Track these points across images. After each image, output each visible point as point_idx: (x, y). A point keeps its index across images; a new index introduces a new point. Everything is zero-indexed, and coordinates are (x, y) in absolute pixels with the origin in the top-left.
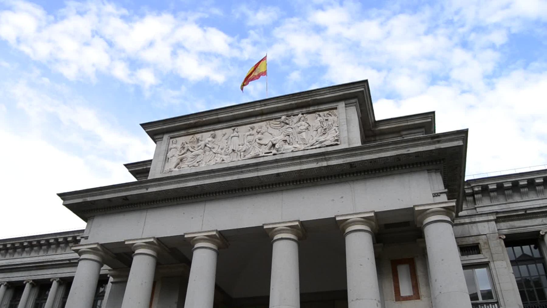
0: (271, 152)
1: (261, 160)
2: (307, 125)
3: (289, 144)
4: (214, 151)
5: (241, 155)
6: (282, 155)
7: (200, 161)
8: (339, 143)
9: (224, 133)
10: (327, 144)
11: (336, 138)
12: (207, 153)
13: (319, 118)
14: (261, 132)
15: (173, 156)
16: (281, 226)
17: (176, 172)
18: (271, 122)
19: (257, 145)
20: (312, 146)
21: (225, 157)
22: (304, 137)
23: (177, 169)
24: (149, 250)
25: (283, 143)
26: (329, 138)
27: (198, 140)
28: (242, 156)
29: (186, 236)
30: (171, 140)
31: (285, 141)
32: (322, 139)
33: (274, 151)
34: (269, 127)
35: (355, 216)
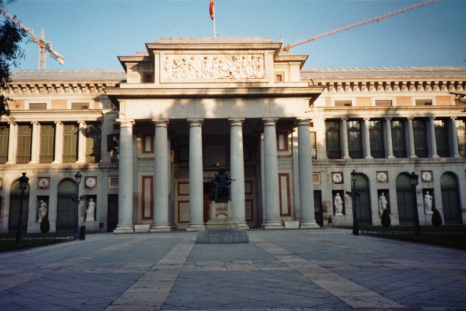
0: (229, 77)
1: (224, 81)
2: (248, 62)
3: (238, 73)
4: (196, 69)
5: (212, 75)
6: (235, 79)
7: (187, 75)
8: (264, 77)
9: (200, 58)
10: (258, 77)
11: (264, 75)
12: (192, 70)
13: (254, 60)
14: (223, 62)
15: (169, 68)
16: (236, 120)
17: (173, 80)
18: (228, 55)
19: (221, 70)
20: (251, 76)
21: (203, 75)
22: (247, 71)
23: (172, 78)
24: (164, 124)
25: (235, 72)
26: (260, 74)
27: (184, 60)
28: (213, 76)
29: (188, 120)
30: (166, 56)
31: (236, 71)
32: (256, 73)
33: (231, 77)
34: (226, 59)
35: (271, 119)
